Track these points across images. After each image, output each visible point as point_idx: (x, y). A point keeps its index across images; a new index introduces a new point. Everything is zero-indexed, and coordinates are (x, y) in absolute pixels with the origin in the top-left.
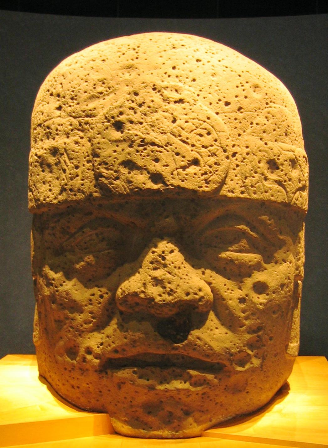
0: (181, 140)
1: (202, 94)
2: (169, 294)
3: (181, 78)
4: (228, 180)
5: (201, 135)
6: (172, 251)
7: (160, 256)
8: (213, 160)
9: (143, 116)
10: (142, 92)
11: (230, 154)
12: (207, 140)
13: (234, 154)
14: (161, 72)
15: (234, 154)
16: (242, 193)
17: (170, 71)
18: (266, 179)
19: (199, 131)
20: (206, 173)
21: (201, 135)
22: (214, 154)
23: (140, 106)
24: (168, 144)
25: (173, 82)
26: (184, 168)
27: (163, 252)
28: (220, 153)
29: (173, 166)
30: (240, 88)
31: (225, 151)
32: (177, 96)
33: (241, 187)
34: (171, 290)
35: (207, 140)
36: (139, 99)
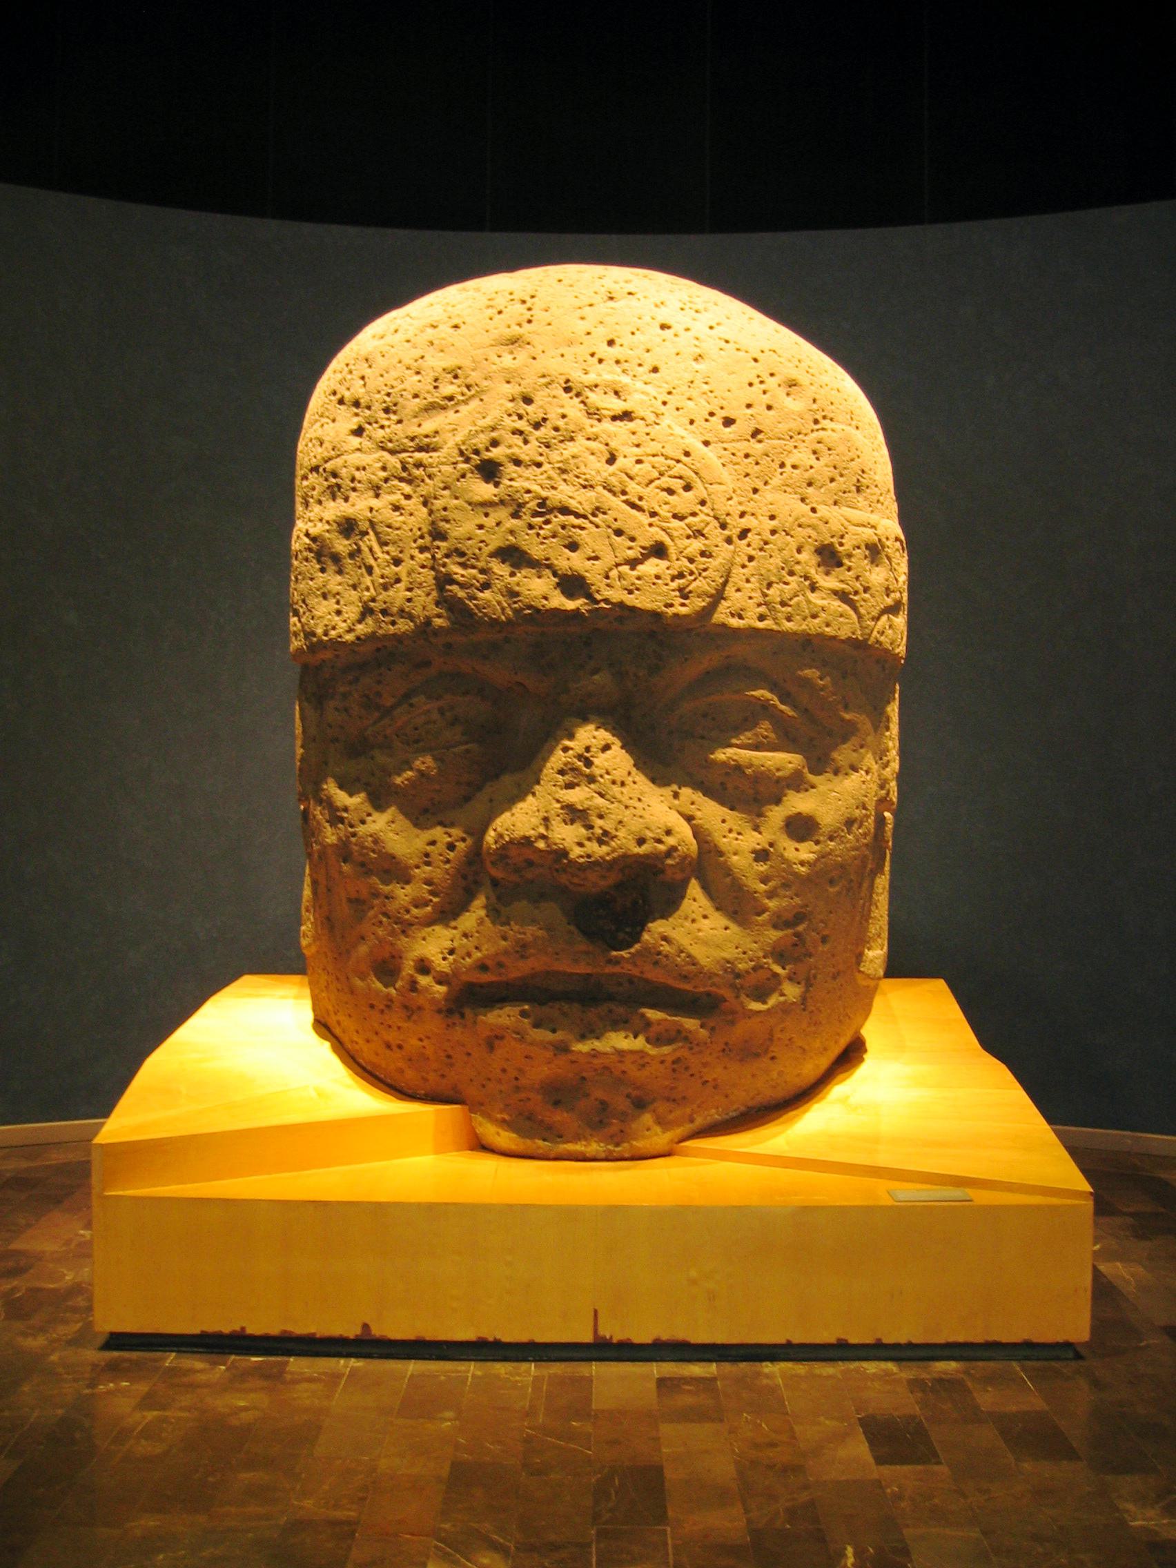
0: (627, 502)
1: (673, 401)
2: (601, 842)
3: (626, 366)
4: (730, 590)
5: (671, 492)
6: (606, 748)
7: (580, 757)
8: (696, 545)
9: (543, 450)
10: (540, 397)
11: (734, 532)
12: (682, 502)
13: (744, 534)
14: (583, 351)
15: (744, 534)
16: (762, 618)
17: (603, 350)
18: (813, 588)
19: (666, 481)
20: (681, 575)
21: (671, 492)
22: (699, 533)
23: (537, 426)
24: (597, 510)
25: (608, 374)
26: (633, 563)
27: (588, 749)
28: (713, 530)
29: (608, 559)
30: (758, 388)
31: (723, 526)
32: (618, 406)
33: (759, 605)
34: (606, 833)
35: (682, 502)
36: (533, 411)
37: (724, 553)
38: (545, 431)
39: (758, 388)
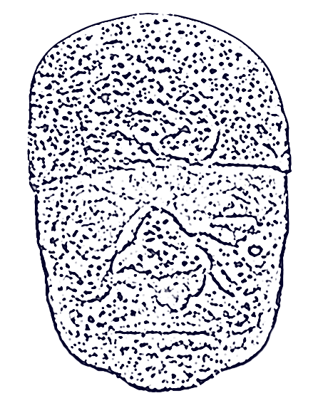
0: (170, 108)
1: (187, 63)
2: (166, 266)
3: (164, 49)
4: (218, 146)
5: (189, 102)
6: (166, 222)
7: (154, 226)
8: (202, 127)
9: (130, 87)
10: (127, 64)
11: (219, 119)
12: (196, 107)
13: (223, 120)
14: (145, 44)
15: (223, 120)
16: (234, 158)
17: (154, 43)
18: (256, 143)
19: (187, 97)
20: (196, 140)
21: (189, 102)
22: (203, 121)
23: (126, 77)
24: (155, 113)
25: (157, 53)
26: (174, 136)
27: (158, 222)
28: (209, 118)
29: (162, 135)
30: (225, 57)
31: (214, 117)
32: (163, 66)
33: (232, 152)
34: (168, 262)
35: (196, 107)
36: (123, 71)
37: (215, 129)
38: (130, 79)
39: (225, 57)
